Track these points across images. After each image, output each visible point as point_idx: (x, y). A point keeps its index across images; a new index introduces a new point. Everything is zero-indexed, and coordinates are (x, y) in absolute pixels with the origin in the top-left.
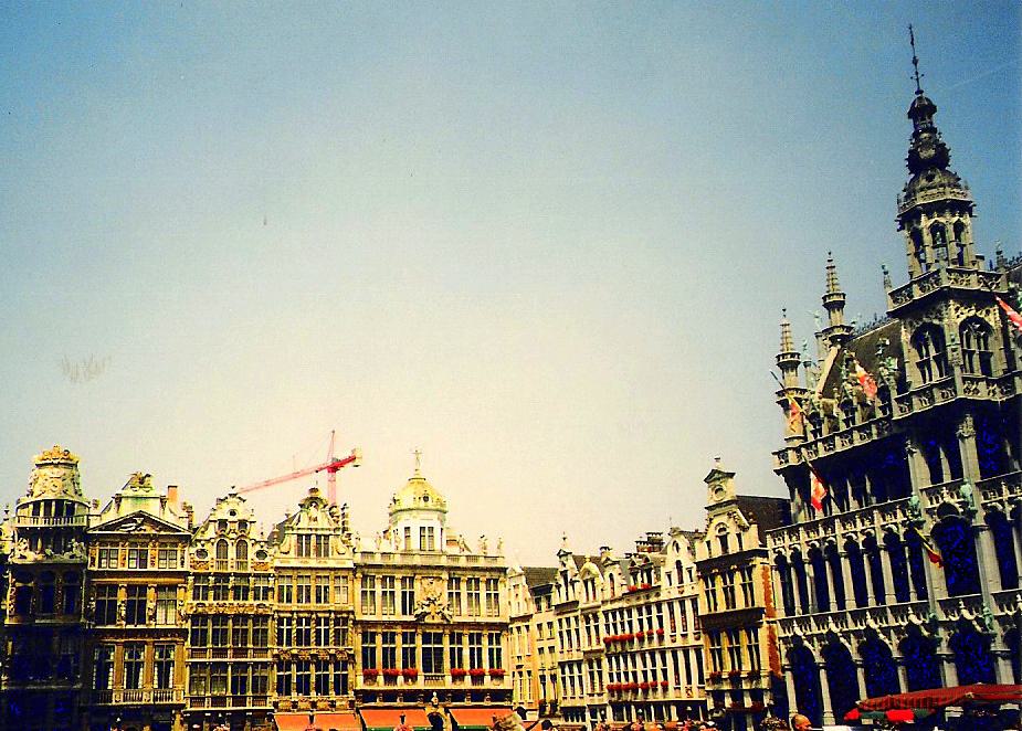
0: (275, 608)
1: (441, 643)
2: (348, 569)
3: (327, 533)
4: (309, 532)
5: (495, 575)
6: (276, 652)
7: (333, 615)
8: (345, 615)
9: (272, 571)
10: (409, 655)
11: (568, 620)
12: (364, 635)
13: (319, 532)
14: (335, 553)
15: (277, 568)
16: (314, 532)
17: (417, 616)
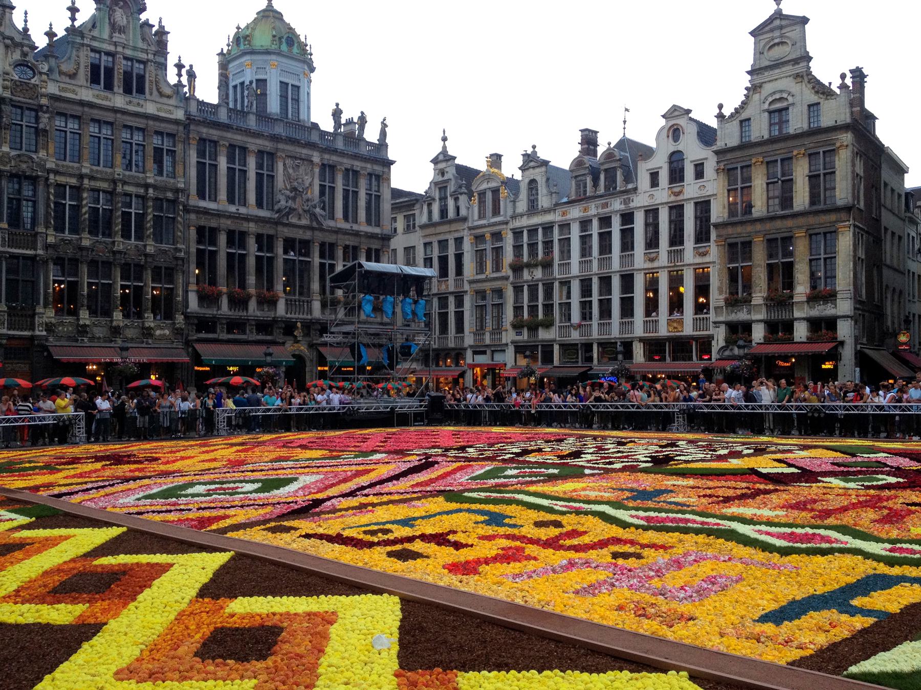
0: (50, 165)
1: (307, 254)
2: (176, 122)
3: (143, 56)
4: (111, 48)
5: (378, 169)
6: (51, 240)
7: (151, 191)
8: (170, 195)
9: (44, 101)
10: (265, 267)
11: (443, 244)
12: (200, 230)
13: (129, 52)
14: (155, 92)
15: (54, 98)
16: (120, 49)
17: (279, 211)
